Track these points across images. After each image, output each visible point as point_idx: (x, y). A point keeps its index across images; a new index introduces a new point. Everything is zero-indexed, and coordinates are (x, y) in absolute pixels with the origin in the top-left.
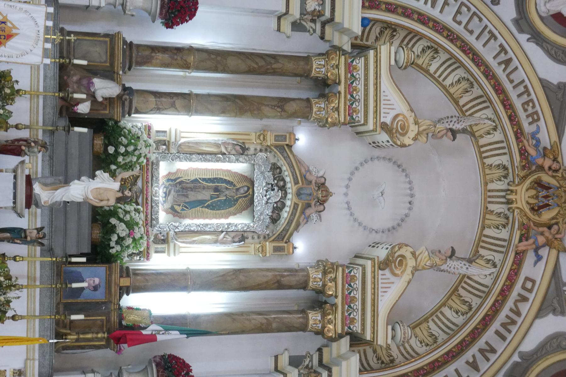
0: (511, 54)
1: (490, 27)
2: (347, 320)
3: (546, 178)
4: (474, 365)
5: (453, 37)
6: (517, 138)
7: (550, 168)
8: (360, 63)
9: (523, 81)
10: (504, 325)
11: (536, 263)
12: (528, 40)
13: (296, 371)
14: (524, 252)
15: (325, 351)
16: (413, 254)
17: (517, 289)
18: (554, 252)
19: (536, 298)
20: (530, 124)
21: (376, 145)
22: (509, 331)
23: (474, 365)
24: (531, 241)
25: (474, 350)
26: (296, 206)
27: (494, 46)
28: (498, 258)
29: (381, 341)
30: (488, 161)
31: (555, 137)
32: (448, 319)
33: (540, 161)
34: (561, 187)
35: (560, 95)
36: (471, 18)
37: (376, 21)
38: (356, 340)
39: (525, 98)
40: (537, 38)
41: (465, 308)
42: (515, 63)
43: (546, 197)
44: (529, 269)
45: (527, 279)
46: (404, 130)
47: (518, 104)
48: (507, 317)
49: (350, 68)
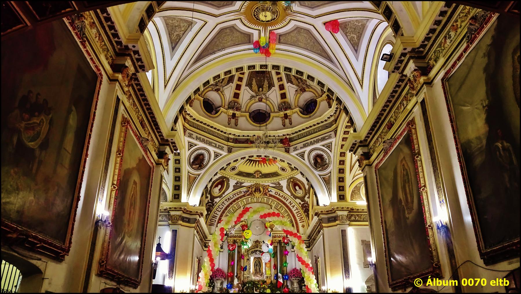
3: (253, 189)
4: (293, 206)
5: (223, 212)
17: (277, 196)
19: (279, 192)
23: (293, 206)
25: (290, 206)
27: (225, 202)
40: (224, 193)
44: (273, 193)
47: (238, 196)
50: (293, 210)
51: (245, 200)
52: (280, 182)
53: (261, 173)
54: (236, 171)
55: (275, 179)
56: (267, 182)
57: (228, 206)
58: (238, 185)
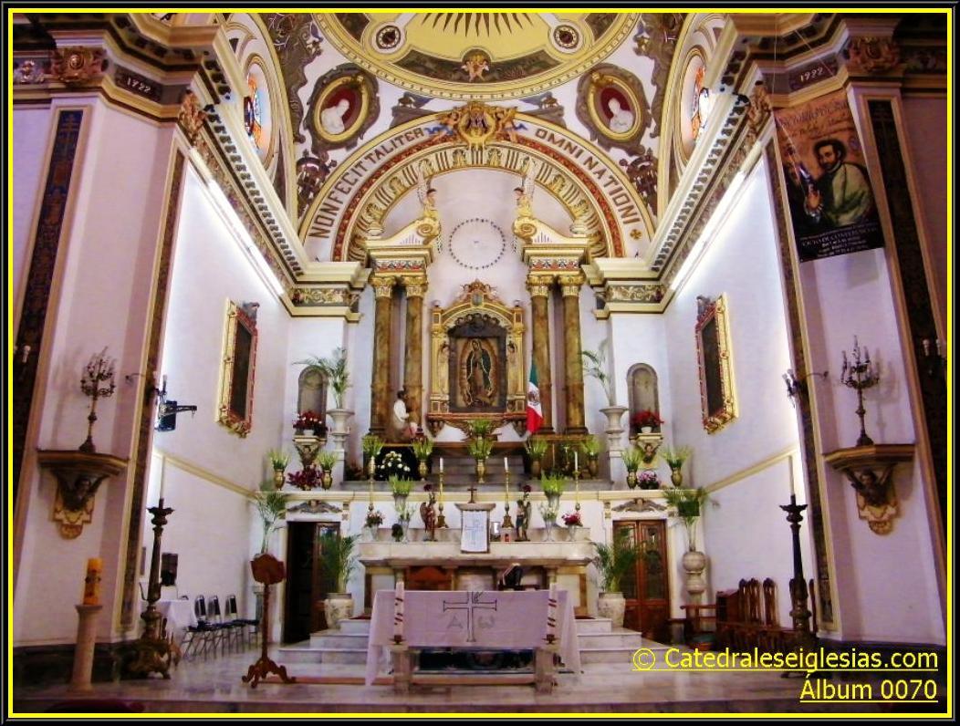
0: (372, 151)
1: (352, 167)
2: (569, 267)
3: (463, 122)
4: (601, 173)
5: (360, 193)
6: (433, 144)
7: (456, 120)
8: (380, 262)
9: (392, 142)
10: (571, 153)
11: (525, 128)
12: (362, 138)
13: (608, 304)
14: (517, 137)
15: (593, 282)
16: (519, 219)
17: (545, 142)
18: (517, 116)
19: (552, 128)
20: (423, 135)
21: (440, 248)
22: (576, 147)
23: (601, 173)
24: (509, 132)
25: (591, 174)
26: (486, 306)
27: (367, 163)
28: (522, 156)
29: (585, 242)
30: (451, 165)
31: (432, 117)
32: (569, 192)
33: (450, 128)
34: (469, 112)
35: (402, 114)
36: (347, 181)
37: (349, 250)
38: (584, 260)
39: (404, 139)
40: (360, 133)
41: (560, 180)
42: (378, 148)
43: (476, 122)
44: (529, 134)
45: (537, 135)
46: (426, 227)
47: (408, 144)
48: (565, 149)
49: (384, 269)
50: (600, 183)
51: (432, 158)
52: (556, 93)
53: (487, 60)
54: (399, 51)
55: (533, 84)
56: (509, 96)
57: (376, 175)
58: (409, 109)
